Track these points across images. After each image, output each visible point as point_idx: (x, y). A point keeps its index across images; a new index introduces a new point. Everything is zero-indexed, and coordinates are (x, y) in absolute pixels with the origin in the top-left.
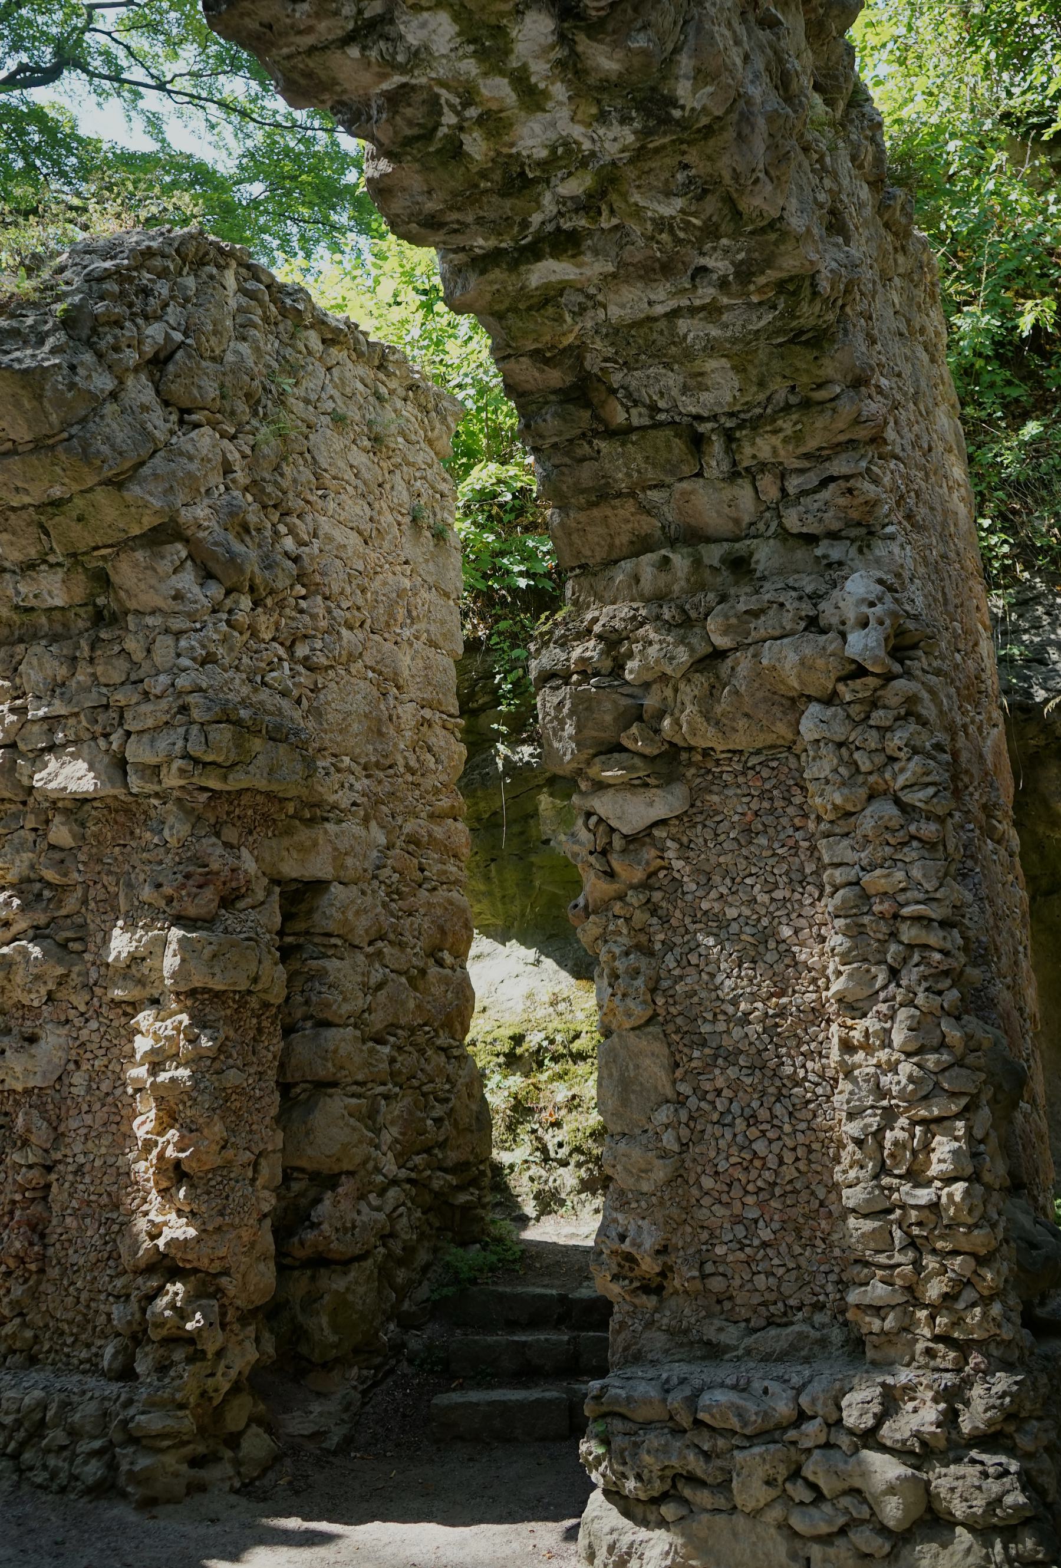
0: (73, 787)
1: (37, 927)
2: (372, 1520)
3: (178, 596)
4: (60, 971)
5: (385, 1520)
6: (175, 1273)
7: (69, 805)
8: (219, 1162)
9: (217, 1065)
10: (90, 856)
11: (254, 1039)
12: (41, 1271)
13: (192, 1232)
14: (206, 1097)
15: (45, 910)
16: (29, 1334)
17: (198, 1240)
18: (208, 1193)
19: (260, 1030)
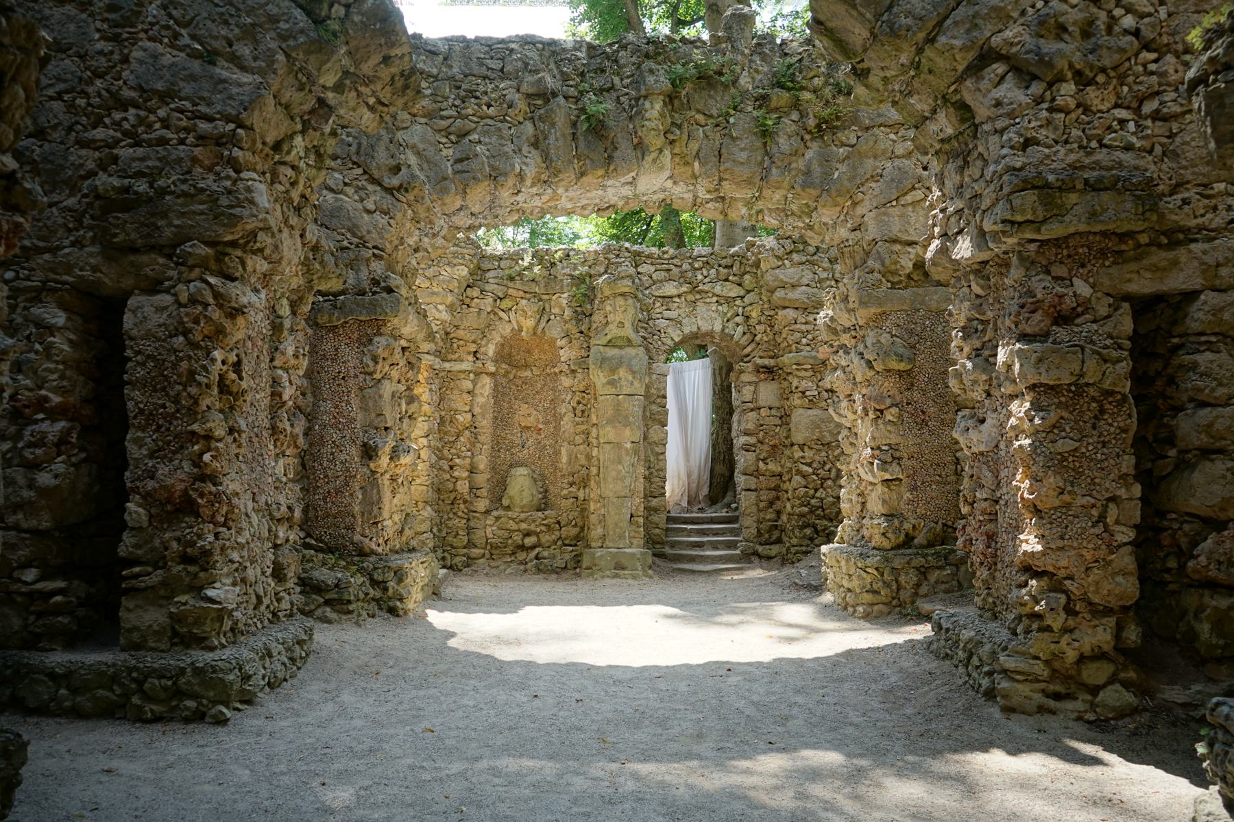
0: (966, 256)
1: (977, 349)
2: (1148, 764)
3: (998, 104)
4: (984, 377)
5: (1157, 767)
6: (1037, 575)
7: (976, 267)
8: (1057, 503)
9: (1051, 436)
10: (995, 299)
11: (1096, 417)
12: (996, 564)
13: (1039, 548)
14: (1041, 458)
15: (978, 338)
16: (991, 600)
17: (1043, 554)
18: (1051, 523)
19: (1102, 411)
